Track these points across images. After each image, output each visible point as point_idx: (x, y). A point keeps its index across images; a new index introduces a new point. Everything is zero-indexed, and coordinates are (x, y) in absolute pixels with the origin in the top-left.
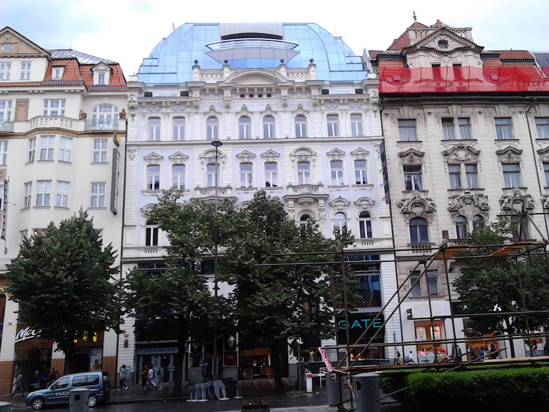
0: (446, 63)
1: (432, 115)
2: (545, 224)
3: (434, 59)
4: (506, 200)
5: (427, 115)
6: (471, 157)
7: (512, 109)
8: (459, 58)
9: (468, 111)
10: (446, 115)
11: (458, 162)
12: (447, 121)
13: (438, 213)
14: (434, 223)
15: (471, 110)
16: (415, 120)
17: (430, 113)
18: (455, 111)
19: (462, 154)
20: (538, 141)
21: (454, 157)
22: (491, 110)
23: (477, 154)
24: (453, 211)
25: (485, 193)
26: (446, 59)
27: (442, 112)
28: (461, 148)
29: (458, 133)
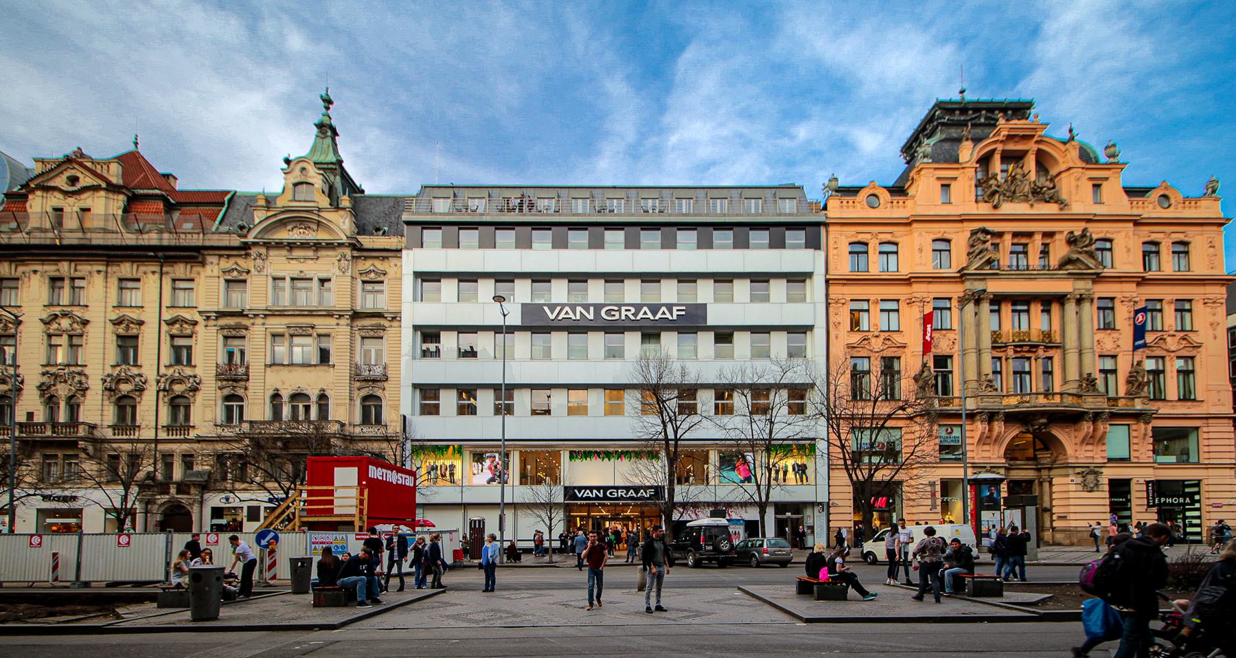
0: (71, 206)
1: (39, 273)
2: (155, 408)
3: (55, 200)
4: (109, 379)
5: (32, 273)
6: (77, 327)
7: (142, 269)
8: (87, 200)
9: (84, 269)
10: (57, 274)
11: (60, 332)
12: (55, 281)
13: (24, 392)
14: (20, 402)
15: (89, 268)
16: (17, 279)
17: (35, 272)
18: (64, 268)
19: (65, 323)
20: (169, 310)
21: (55, 326)
22: (115, 268)
23: (85, 323)
24: (43, 388)
25: (87, 371)
26: (71, 200)
27: (50, 269)
28: (65, 315)
29: (65, 296)
